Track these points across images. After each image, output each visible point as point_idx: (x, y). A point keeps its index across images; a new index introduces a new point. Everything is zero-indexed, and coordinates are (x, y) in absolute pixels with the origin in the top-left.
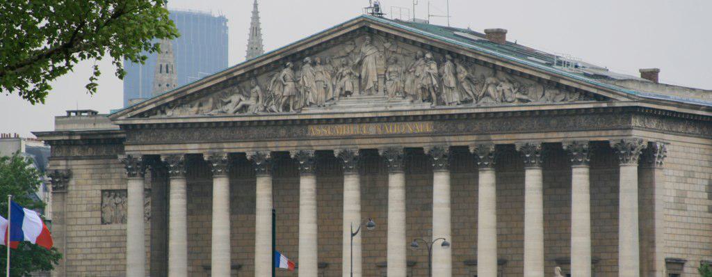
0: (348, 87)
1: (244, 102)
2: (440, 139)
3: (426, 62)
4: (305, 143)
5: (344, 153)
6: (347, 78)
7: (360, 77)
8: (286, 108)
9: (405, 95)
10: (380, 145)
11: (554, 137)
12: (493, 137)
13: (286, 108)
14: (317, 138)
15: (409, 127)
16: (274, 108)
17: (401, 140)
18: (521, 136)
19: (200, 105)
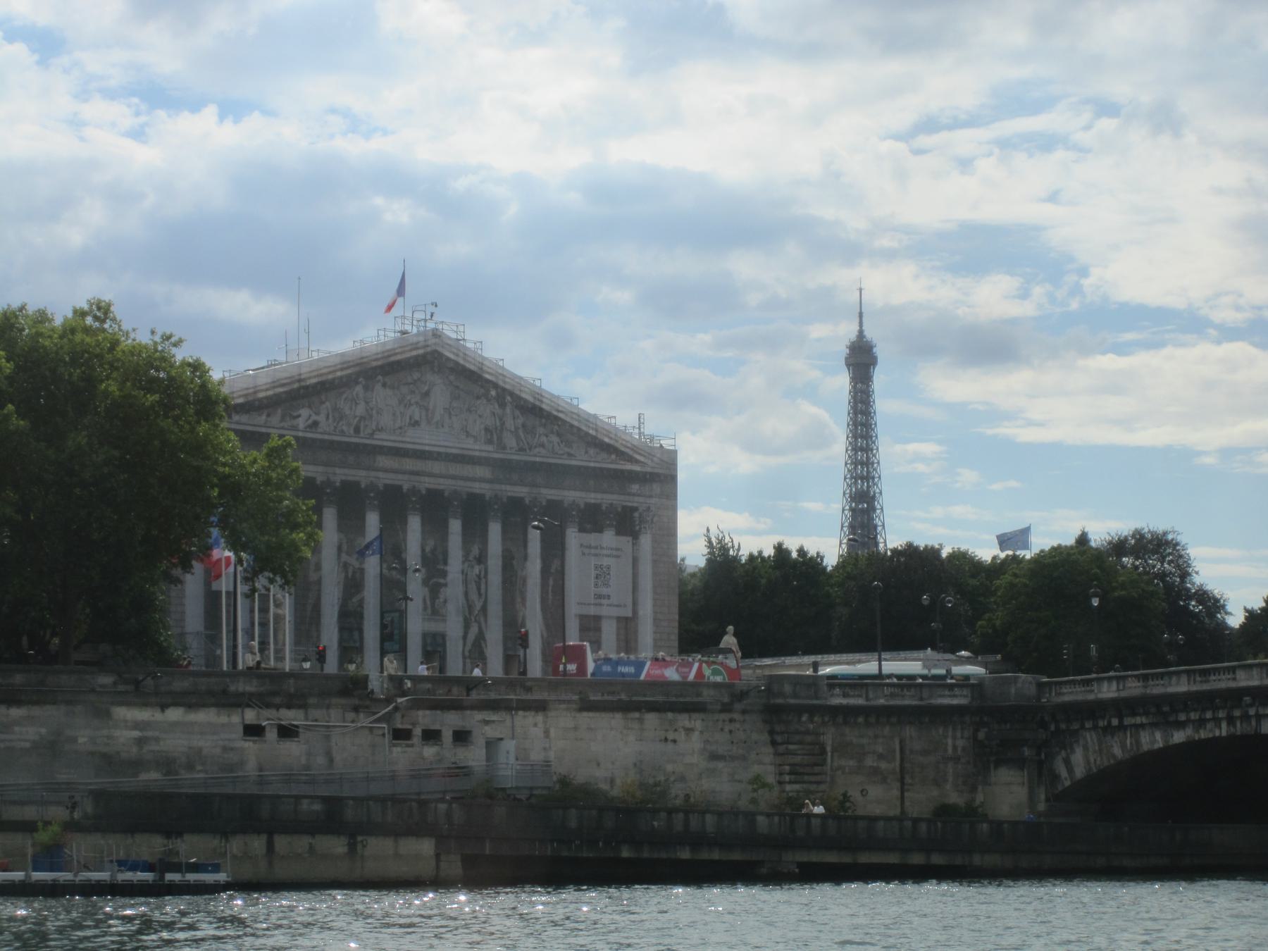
0: (417, 417)
1: (314, 417)
2: (497, 487)
3: (489, 400)
4: (373, 474)
5: (414, 491)
6: (414, 407)
7: (427, 410)
8: (357, 430)
9: (468, 434)
10: (445, 485)
11: (593, 498)
12: (544, 491)
13: (357, 430)
14: (386, 471)
15: (468, 470)
16: (345, 428)
17: (460, 483)
18: (566, 493)
19: (268, 415)
